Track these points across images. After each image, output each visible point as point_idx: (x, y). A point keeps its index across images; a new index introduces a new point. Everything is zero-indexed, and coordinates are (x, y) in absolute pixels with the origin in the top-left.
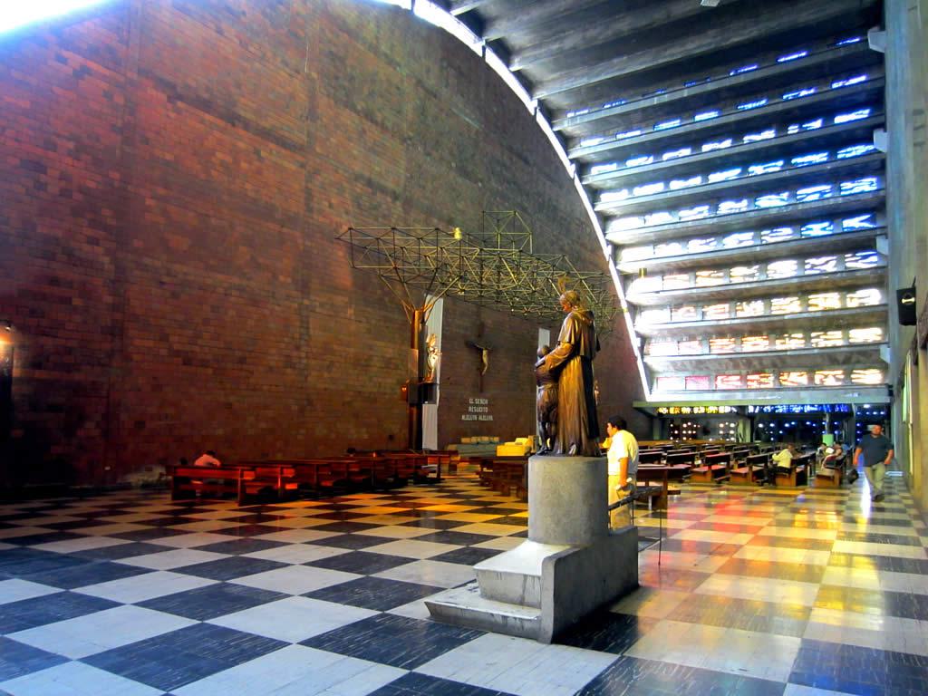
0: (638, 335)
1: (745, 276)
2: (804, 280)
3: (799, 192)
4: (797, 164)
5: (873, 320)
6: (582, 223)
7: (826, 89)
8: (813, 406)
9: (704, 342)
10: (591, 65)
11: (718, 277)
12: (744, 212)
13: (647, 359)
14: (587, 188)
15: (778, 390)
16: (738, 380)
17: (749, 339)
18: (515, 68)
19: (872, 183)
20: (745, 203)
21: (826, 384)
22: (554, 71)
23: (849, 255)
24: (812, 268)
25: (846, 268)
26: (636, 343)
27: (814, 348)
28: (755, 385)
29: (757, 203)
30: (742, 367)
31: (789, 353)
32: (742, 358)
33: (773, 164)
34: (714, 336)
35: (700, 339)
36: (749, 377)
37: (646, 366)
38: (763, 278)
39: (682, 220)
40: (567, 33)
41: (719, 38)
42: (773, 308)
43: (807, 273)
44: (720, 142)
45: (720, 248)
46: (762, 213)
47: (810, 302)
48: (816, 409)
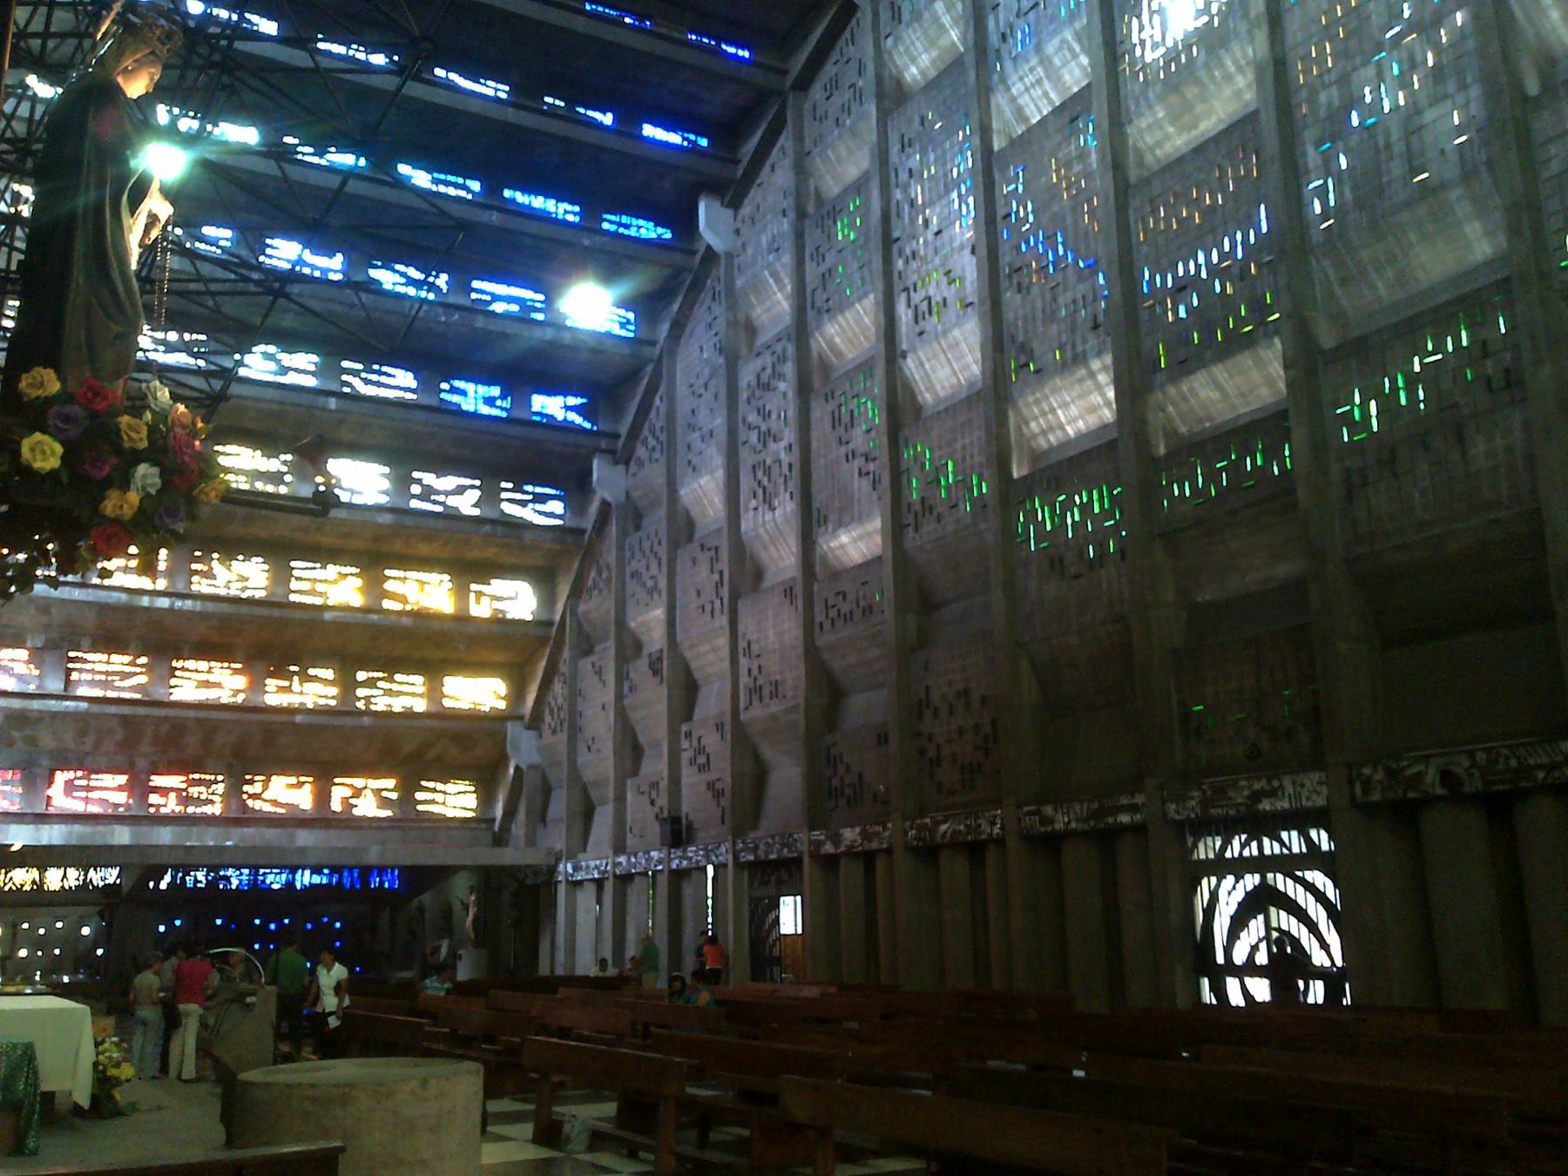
2: (409, 521)
3: (476, 284)
4: (513, 200)
5: (499, 657)
7: (676, 35)
8: (316, 870)
9: (49, 658)
16: (120, 788)
17: (191, 664)
19: (628, 322)
20: (339, 257)
21: (356, 812)
23: (510, 485)
27: (360, 713)
28: (171, 805)
30: (146, 748)
31: (299, 719)
32: (166, 719)
33: (460, 180)
34: (86, 643)
36: (158, 781)
42: (294, 585)
43: (415, 504)
44: (372, 49)
47: (389, 586)
48: (325, 881)
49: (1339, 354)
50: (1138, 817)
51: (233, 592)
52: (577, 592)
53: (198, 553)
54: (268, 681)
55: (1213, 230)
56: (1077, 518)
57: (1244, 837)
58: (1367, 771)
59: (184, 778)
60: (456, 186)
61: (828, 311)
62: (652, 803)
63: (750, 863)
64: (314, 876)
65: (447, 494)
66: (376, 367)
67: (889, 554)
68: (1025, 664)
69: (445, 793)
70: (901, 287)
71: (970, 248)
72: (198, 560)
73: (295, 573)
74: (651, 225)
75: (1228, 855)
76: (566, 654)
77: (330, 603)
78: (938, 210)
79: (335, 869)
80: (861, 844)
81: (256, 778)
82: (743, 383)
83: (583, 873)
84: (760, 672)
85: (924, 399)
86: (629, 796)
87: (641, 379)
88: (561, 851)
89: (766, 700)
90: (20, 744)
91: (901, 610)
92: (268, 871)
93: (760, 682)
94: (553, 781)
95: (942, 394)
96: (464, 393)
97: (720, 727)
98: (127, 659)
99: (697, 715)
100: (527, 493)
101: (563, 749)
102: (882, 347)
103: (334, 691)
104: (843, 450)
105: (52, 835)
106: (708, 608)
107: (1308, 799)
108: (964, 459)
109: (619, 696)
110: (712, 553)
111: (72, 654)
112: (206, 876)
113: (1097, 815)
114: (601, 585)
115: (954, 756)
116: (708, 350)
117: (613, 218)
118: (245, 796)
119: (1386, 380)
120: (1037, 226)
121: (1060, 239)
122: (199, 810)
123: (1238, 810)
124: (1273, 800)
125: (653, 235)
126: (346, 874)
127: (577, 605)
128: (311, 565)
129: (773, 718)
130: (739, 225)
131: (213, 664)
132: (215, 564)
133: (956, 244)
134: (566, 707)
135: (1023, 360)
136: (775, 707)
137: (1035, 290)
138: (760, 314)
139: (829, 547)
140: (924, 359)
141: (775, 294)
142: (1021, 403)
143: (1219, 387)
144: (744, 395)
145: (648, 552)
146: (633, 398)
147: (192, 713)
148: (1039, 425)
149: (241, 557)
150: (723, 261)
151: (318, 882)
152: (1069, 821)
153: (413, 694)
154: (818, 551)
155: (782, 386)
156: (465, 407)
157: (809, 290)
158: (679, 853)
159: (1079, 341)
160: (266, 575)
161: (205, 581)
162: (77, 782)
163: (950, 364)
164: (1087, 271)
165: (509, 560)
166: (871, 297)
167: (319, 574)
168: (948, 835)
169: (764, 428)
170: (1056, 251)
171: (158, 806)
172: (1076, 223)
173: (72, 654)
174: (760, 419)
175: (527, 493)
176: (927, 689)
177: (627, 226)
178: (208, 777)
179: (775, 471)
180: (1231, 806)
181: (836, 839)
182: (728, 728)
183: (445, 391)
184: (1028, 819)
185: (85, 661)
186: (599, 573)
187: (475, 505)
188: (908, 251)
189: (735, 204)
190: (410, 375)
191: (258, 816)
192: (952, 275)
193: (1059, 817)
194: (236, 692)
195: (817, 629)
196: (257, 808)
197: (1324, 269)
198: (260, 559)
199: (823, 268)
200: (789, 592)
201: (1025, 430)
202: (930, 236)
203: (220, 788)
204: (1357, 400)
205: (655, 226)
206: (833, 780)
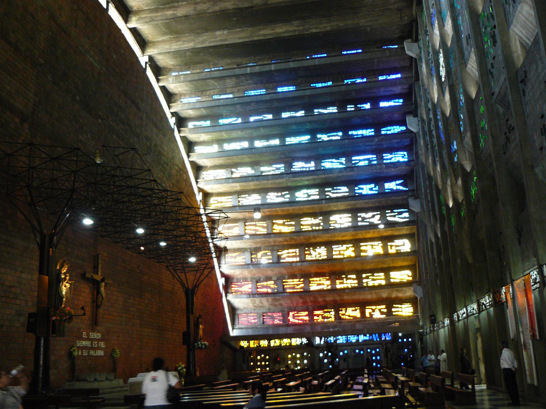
0: (223, 275)
1: (312, 225)
3: (353, 158)
4: (352, 135)
6: (181, 170)
7: (374, 79)
8: (365, 335)
9: (279, 282)
10: (198, 33)
11: (291, 225)
12: (313, 171)
13: (230, 297)
14: (184, 139)
16: (306, 316)
17: (315, 279)
18: (132, 25)
19: (405, 156)
20: (312, 164)
22: (164, 34)
23: (389, 211)
26: (221, 281)
27: (365, 287)
28: (320, 319)
29: (322, 164)
33: (335, 134)
35: (276, 279)
36: (316, 312)
37: (229, 302)
38: (326, 227)
39: (263, 174)
40: (180, 3)
41: (301, 28)
42: (334, 253)
43: (360, 224)
44: (296, 111)
45: (293, 200)
47: (362, 248)
51: (317, 258)
53: (307, 249)
54: (337, 281)
59: (322, 311)
60: (334, 136)
65: (369, 218)
66: (335, 188)
69: (401, 308)
72: (307, 250)
73: (334, 249)
77: (345, 256)
79: (371, 335)
90: (279, 306)
92: (350, 336)
96: (362, 189)
98: (298, 280)
100: (396, 212)
103: (356, 281)
105: (290, 330)
111: (284, 281)
117: (385, 129)
118: (340, 315)
125: (399, 130)
128: (338, 246)
131: (321, 278)
132: (311, 251)
149: (318, 247)
153: (381, 279)
161: (309, 256)
162: (295, 315)
171: (317, 320)
173: (284, 281)
175: (396, 212)
177: (390, 130)
178: (329, 310)
185: (287, 282)
187: (378, 220)
194: (328, 286)
196: (344, 318)
198: (324, 247)
203: (333, 313)
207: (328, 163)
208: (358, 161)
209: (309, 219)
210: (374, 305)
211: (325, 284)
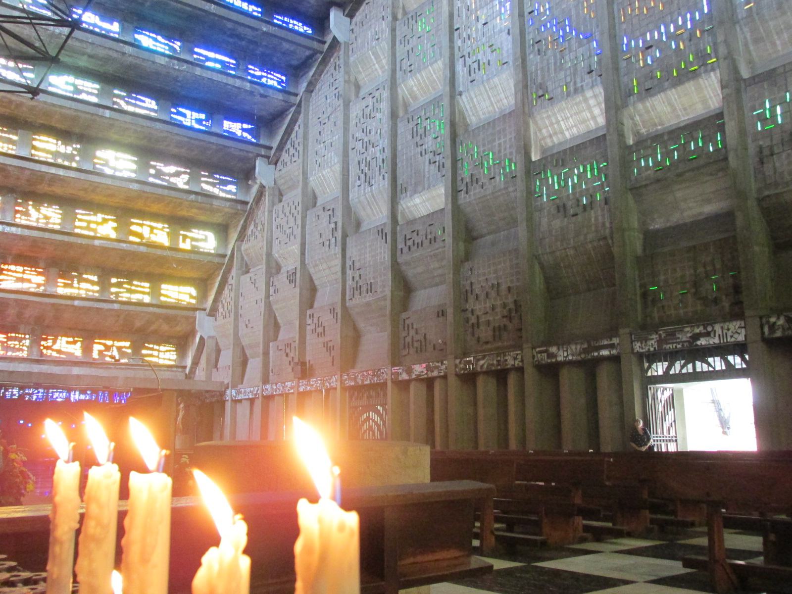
1: (56, 154)
2: (148, 189)
3: (196, 50)
8: (83, 392)
11: (10, 141)
15: (37, 361)
17: (13, 267)
19: (282, 82)
23: (207, 174)
24: (155, 176)
25: (202, 188)
29: (137, 36)
31: (76, 303)
38: (87, 167)
42: (77, 223)
43: (151, 180)
46: (146, 55)
49: (757, 79)
50: (614, 352)
51: (41, 225)
52: (242, 237)
53: (20, 201)
54: (59, 280)
55: (671, 14)
56: (576, 181)
57: (683, 362)
58: (773, 320)
59: (5, 336)
61: (410, 71)
62: (287, 355)
63: (351, 387)
64: (81, 395)
66: (134, 95)
67: (450, 206)
68: (537, 268)
69: (159, 351)
70: (460, 55)
71: (507, 31)
72: (19, 205)
73: (79, 216)
74: (300, 24)
75: (672, 372)
76: (234, 272)
77: (98, 235)
78: (485, 11)
79: (95, 391)
80: (426, 374)
81: (49, 337)
82: (353, 115)
83: (242, 395)
84: (360, 278)
85: (470, 120)
86: (271, 352)
87: (287, 115)
88: (228, 384)
89: (364, 293)
91: (455, 238)
93: (360, 283)
94: (221, 344)
95: (482, 117)
96: (184, 116)
97: (333, 311)
99: (316, 305)
101: (231, 328)
102: (448, 89)
104: (419, 149)
106: (327, 243)
107: (732, 337)
108: (500, 151)
109: (268, 296)
110: (331, 212)
112: (19, 392)
113: (585, 351)
114: (257, 233)
115: (488, 323)
116: (330, 98)
117: (280, 18)
119: (788, 94)
120: (553, 16)
121: (567, 23)
122: (14, 354)
123: (683, 345)
124: (707, 339)
126: (100, 394)
127: (241, 246)
128: (87, 212)
129: (368, 304)
130: (353, 26)
131: (26, 268)
132: (30, 208)
133: (496, 30)
134: (232, 303)
135: (540, 93)
136: (369, 298)
137: (549, 53)
138: (363, 78)
139: (407, 206)
140: (473, 96)
141: (374, 65)
142: (538, 118)
143: (670, 104)
144: (353, 123)
145: (288, 214)
146: (281, 127)
147: (13, 296)
148: (548, 131)
149: (46, 205)
150: (342, 47)
151: (83, 398)
152: (568, 355)
154: (400, 208)
155: (379, 115)
156: (185, 123)
157: (398, 60)
158: (305, 382)
159: (578, 80)
160: (60, 216)
161: (23, 217)
163: (489, 98)
164: (585, 41)
165: (202, 218)
166: (440, 63)
167: (92, 218)
168: (485, 366)
169: (366, 139)
170: (564, 30)
172: (578, 14)
174: (364, 135)
175: (216, 179)
176: (471, 284)
179: (373, 164)
180: (678, 343)
181: (409, 371)
182: (339, 310)
183: (174, 113)
184: (539, 355)
186: (256, 226)
188: (465, 35)
189: (351, 16)
190: (154, 102)
191: (49, 359)
192: (494, 48)
193: (561, 353)
194: (39, 285)
195: (399, 252)
197: (744, 34)
198: (57, 207)
199: (408, 47)
200: (381, 232)
201: (538, 134)
202: (480, 25)
203: (27, 342)
204: (768, 106)
205: (303, 25)
206: (407, 339)
207: (146, 38)
208: (204, 59)
209: (52, 140)
210: (109, 339)
211: (33, 281)
